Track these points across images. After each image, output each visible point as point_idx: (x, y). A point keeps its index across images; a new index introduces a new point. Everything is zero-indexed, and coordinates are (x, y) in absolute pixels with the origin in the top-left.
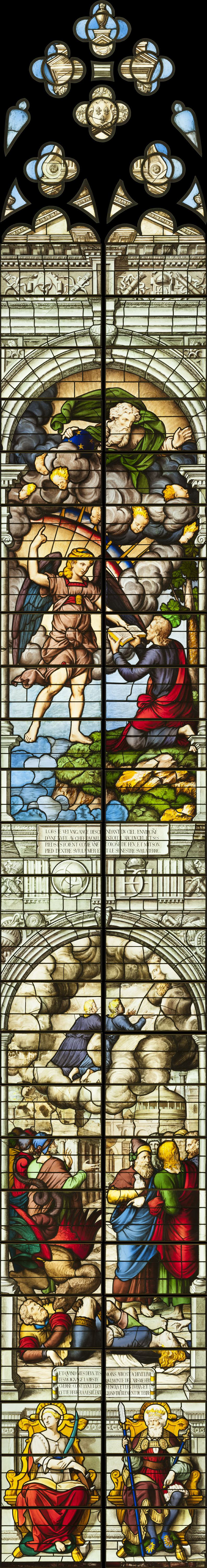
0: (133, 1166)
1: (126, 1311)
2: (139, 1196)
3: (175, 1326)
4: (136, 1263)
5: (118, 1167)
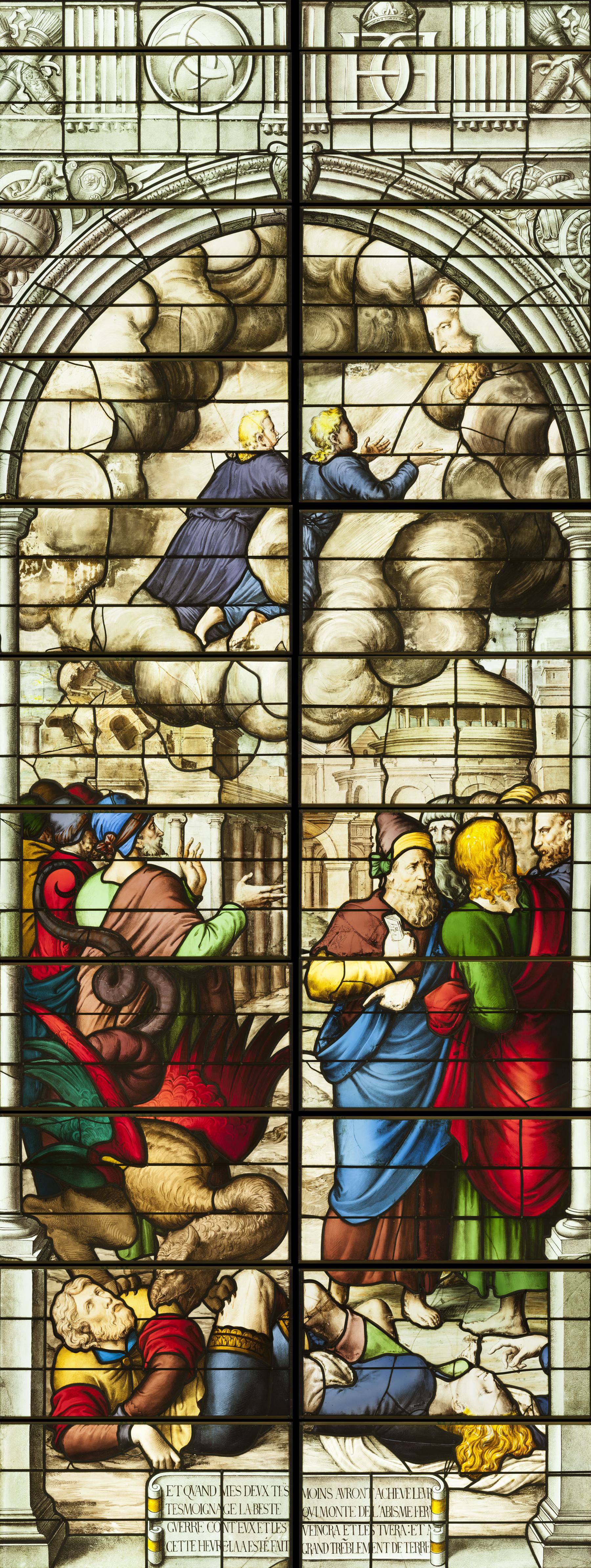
0: (382, 890)
1: (360, 1309)
2: (399, 977)
3: (502, 1355)
4: (389, 1173)
5: (337, 897)
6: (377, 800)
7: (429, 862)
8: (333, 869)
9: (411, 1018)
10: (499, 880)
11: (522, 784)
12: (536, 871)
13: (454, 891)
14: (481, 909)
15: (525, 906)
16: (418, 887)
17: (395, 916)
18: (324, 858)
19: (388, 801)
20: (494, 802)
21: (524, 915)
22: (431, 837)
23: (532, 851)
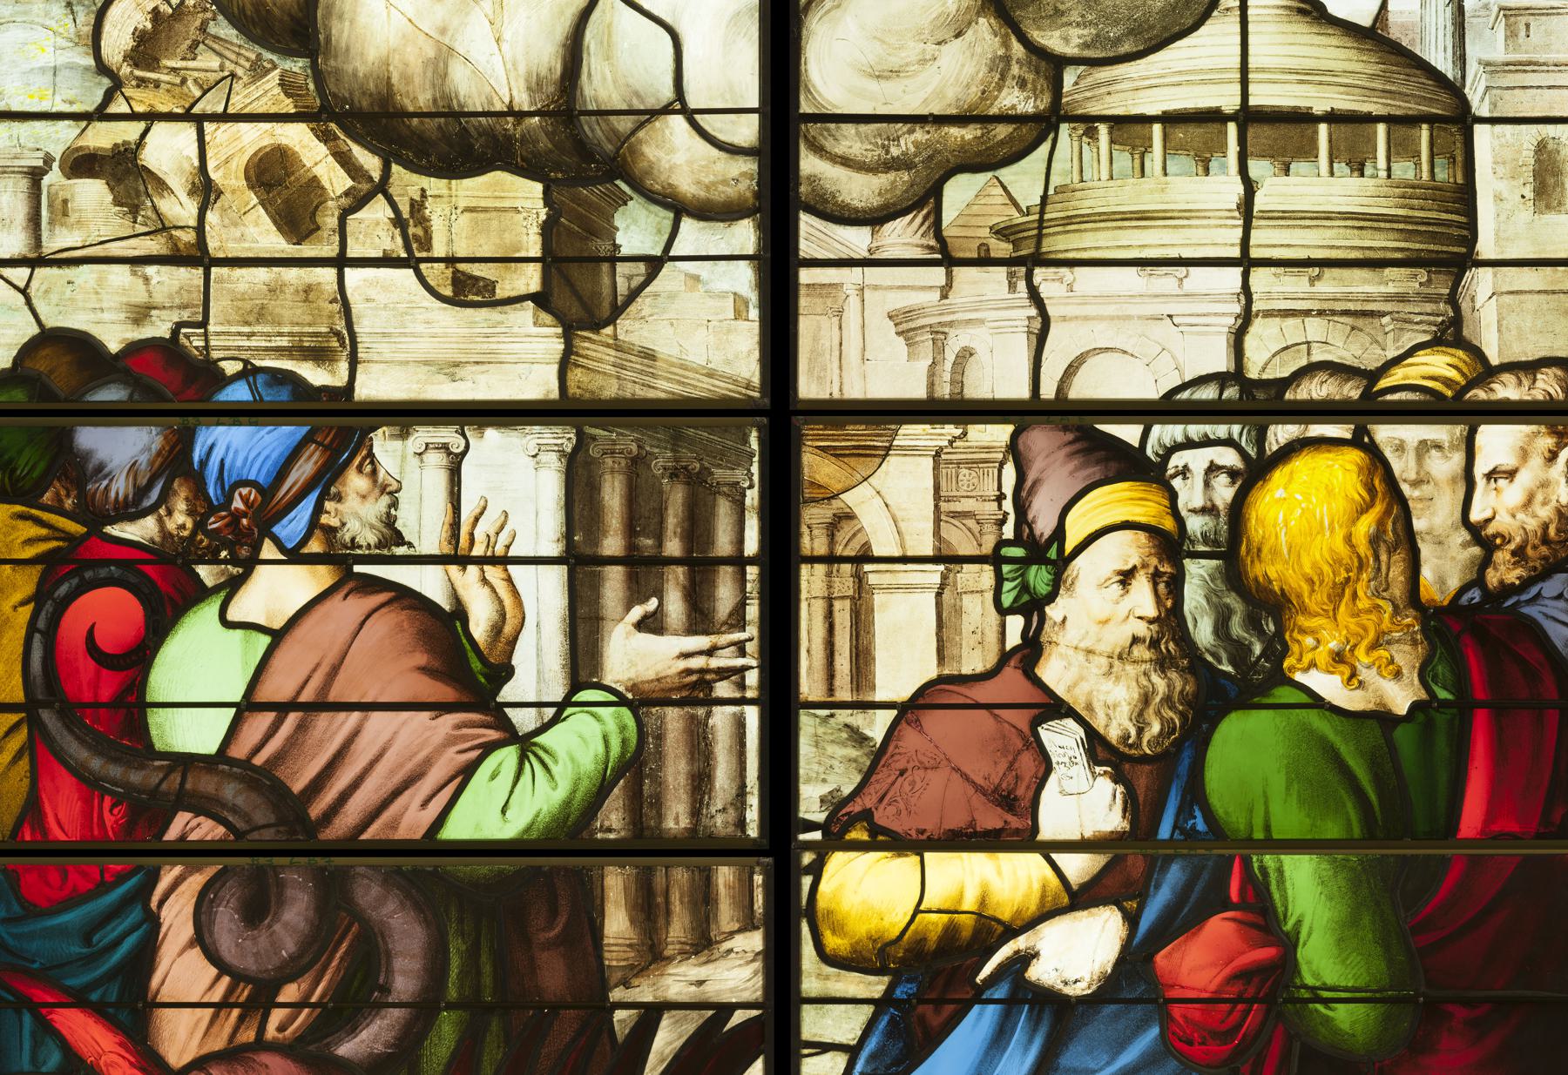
0: (1032, 649)
2: (1080, 898)
6: (1020, 390)
7: (1166, 568)
8: (889, 588)
9: (1116, 1017)
10: (1370, 621)
11: (1436, 342)
12: (1475, 594)
13: (1239, 652)
14: (1317, 702)
15: (1443, 694)
16: (1136, 640)
17: (1070, 723)
18: (865, 557)
19: (1048, 391)
20: (1355, 394)
21: (1441, 719)
22: (1173, 496)
23: (1464, 535)
